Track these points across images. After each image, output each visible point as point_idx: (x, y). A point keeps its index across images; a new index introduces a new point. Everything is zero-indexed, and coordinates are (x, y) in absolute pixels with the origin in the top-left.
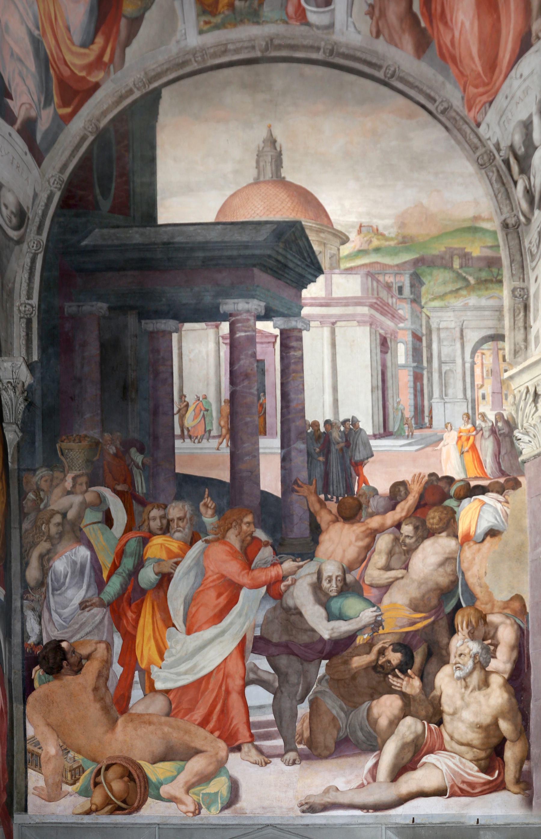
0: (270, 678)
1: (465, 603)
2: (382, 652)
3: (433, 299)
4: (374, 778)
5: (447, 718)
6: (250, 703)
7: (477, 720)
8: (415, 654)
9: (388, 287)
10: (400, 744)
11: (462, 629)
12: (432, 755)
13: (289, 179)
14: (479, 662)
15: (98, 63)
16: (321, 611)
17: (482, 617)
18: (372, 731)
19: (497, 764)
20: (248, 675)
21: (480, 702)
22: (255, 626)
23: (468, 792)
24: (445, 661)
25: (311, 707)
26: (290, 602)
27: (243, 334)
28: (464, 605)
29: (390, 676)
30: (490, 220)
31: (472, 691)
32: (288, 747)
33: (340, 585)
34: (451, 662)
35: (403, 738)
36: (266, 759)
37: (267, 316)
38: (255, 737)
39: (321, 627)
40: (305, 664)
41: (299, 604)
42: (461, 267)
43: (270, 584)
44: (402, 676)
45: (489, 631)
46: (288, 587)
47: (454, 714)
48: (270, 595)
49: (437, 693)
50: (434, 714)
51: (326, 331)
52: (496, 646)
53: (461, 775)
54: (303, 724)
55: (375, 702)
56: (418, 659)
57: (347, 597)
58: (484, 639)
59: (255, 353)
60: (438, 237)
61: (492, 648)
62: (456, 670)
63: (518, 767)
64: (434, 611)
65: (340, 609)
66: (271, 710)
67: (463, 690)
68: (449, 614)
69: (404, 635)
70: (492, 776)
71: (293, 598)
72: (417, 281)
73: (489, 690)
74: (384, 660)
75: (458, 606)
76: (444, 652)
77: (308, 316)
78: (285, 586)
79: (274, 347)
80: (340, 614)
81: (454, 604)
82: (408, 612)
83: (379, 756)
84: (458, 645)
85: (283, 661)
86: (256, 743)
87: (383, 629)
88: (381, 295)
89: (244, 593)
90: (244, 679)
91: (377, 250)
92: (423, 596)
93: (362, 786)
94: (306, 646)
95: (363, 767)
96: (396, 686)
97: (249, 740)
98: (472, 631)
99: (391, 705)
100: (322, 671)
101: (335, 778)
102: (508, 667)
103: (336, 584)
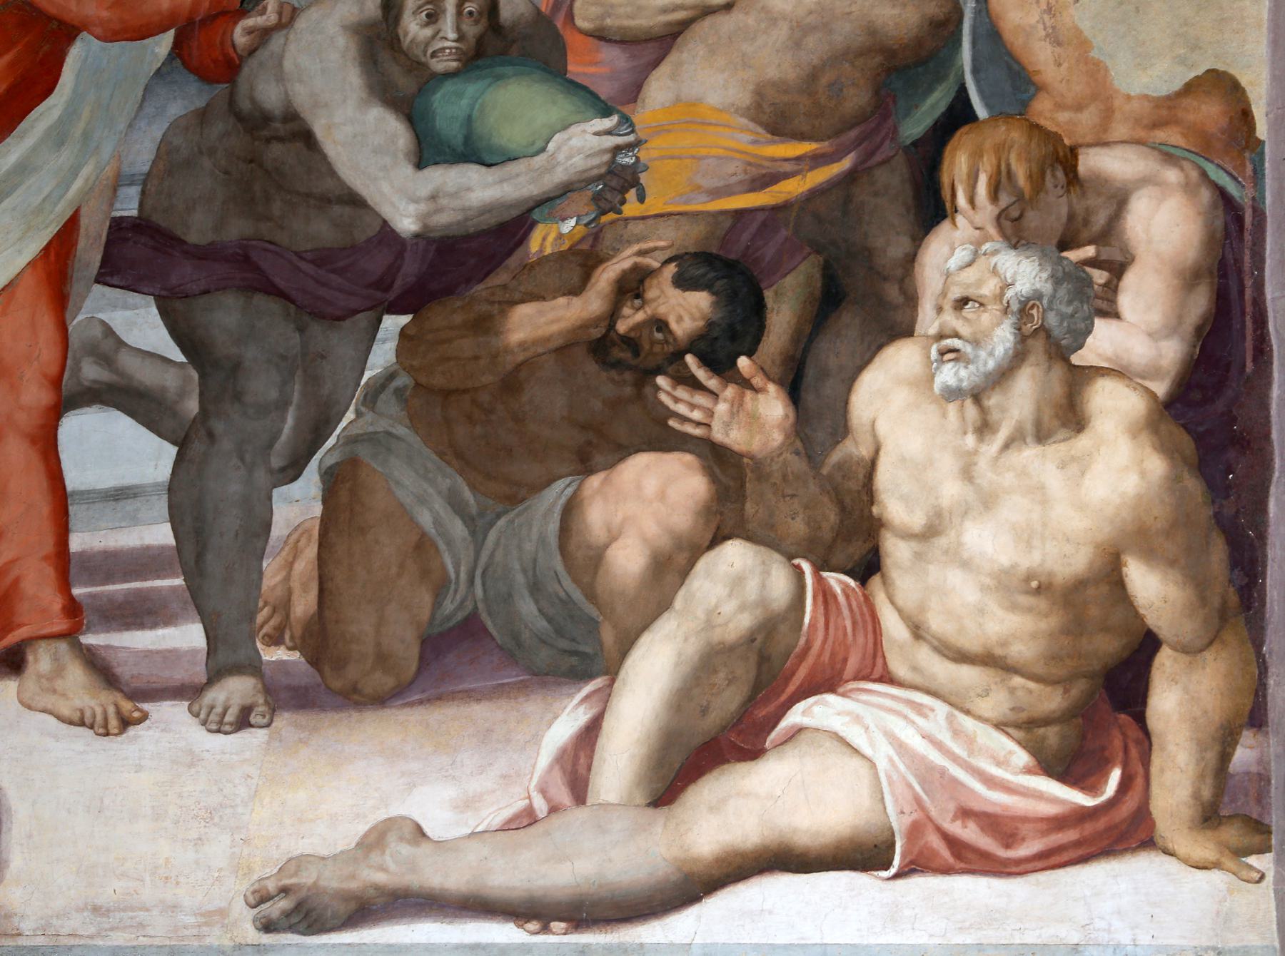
0: (169, 380)
1: (988, 105)
2: (632, 286)
4: (579, 788)
5: (896, 551)
6: (74, 479)
7: (1030, 560)
8: (768, 295)
10: (693, 648)
11: (972, 201)
12: (830, 698)
14: (1043, 330)
16: (390, 128)
17: (1062, 159)
18: (577, 595)
19: (1118, 742)
20: (77, 369)
21: (1042, 488)
22: (118, 182)
23: (985, 855)
24: (894, 324)
25: (329, 496)
26: (269, 95)
28: (981, 112)
29: (661, 381)
31: (1006, 446)
32: (223, 657)
33: (472, 30)
34: (919, 329)
35: (709, 625)
36: (127, 706)
38: (88, 617)
39: (386, 187)
40: (316, 328)
41: (301, 96)
43: (190, 22)
44: (712, 383)
45: (1089, 212)
46: (264, 35)
47: (930, 533)
48: (187, 66)
49: (855, 448)
50: (844, 534)
52: (1118, 270)
53: (955, 782)
54: (290, 565)
55: (595, 481)
56: (782, 317)
57: (499, 78)
58: (1064, 245)
61: (1099, 276)
62: (942, 362)
63: (1211, 756)
64: (853, 134)
65: (469, 119)
66: (161, 506)
67: (970, 440)
68: (915, 144)
69: (728, 223)
70: (1091, 788)
71: (280, 77)
73: (1083, 442)
74: (640, 316)
75: (959, 115)
76: (892, 292)
78: (250, 31)
80: (468, 139)
81: (942, 107)
82: (747, 137)
83: (605, 698)
84: (953, 263)
85: (225, 316)
86: (89, 639)
87: (641, 198)
89: (78, 55)
90: (57, 382)
92: (813, 75)
93: (526, 819)
94: (323, 258)
95: (536, 739)
96: (684, 419)
97: (61, 625)
98: (1015, 214)
99: (662, 496)
100: (382, 355)
101: (411, 786)
102: (1171, 353)
103: (458, 29)
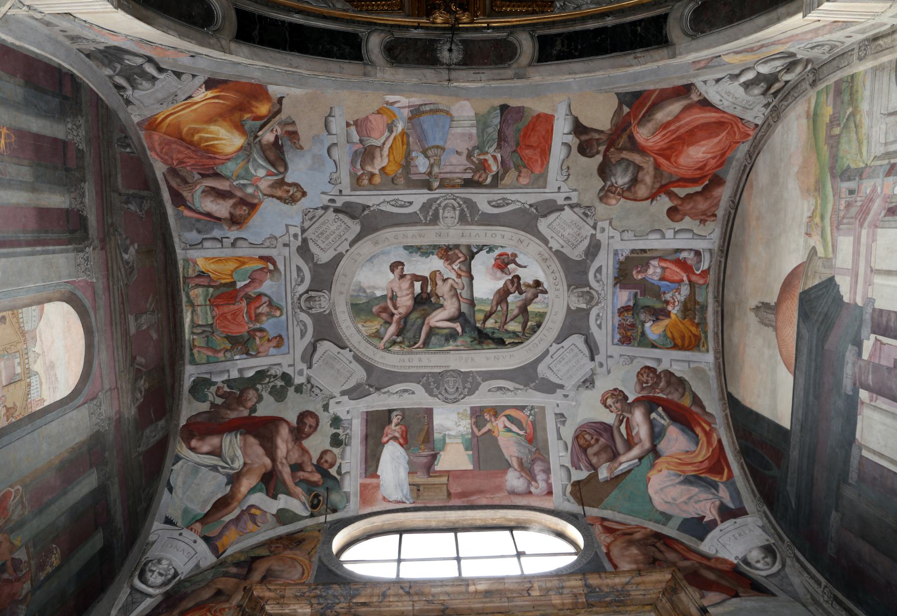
3: (861, 153)
9: (849, 205)
13: (775, 300)
15: (708, 435)
27: (870, 377)
30: (809, 100)
37: (858, 344)
42: (839, 125)
51: (878, 280)
59: (888, 368)
60: (818, 153)
72: (847, 174)
77: (863, 298)
79: (885, 344)
88: (853, 214)
91: (822, 218)
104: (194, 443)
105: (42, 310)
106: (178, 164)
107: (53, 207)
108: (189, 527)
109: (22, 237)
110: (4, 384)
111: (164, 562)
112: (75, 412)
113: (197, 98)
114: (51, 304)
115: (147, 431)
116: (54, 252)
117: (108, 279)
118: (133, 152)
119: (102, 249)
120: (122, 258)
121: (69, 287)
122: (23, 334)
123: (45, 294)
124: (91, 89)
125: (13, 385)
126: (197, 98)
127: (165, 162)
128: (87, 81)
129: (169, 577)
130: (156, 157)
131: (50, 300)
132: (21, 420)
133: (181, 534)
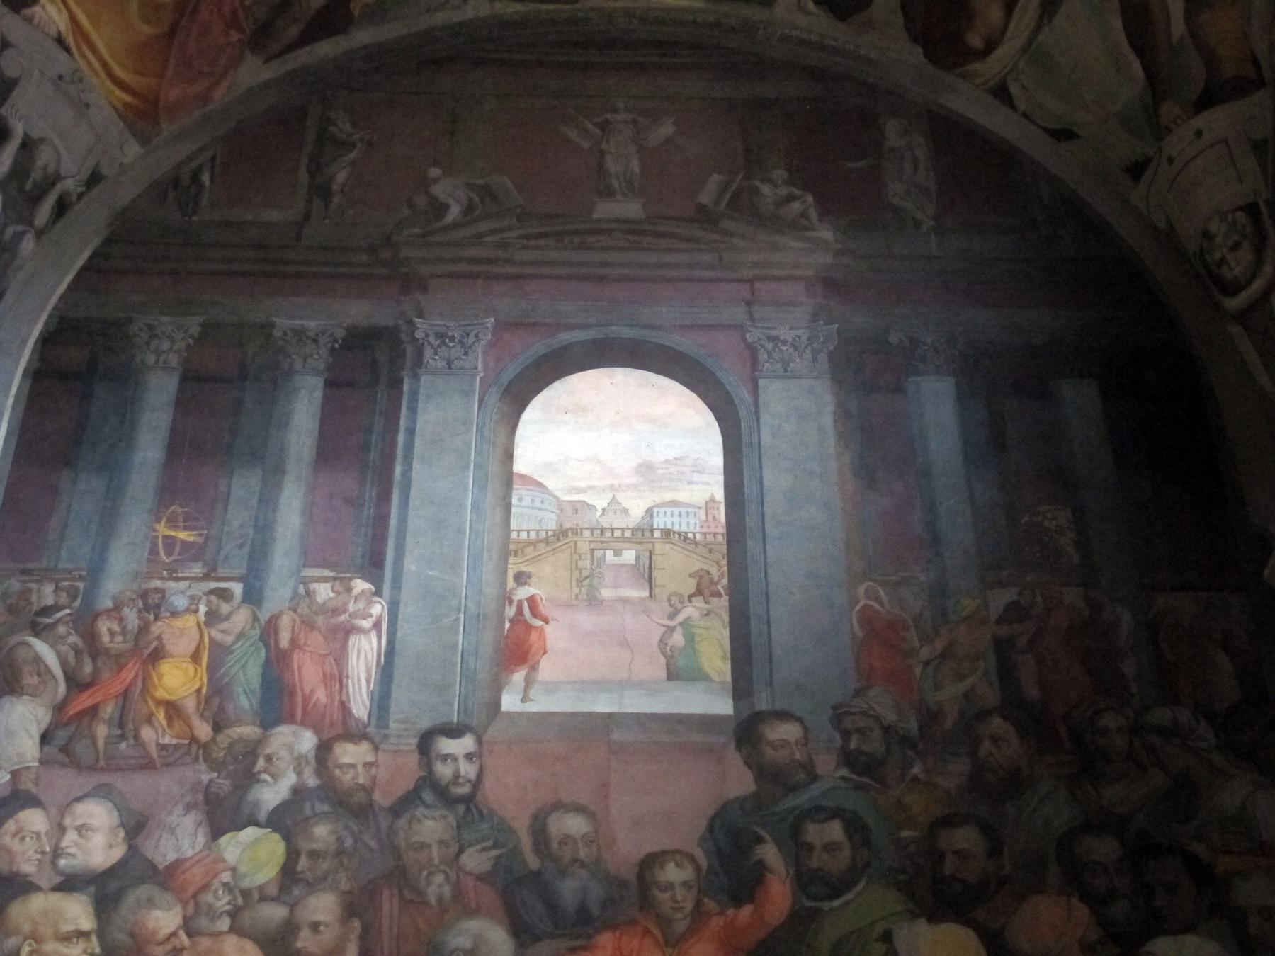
104: (975, 40)
105: (528, 480)
106: (241, 30)
107: (317, 425)
108: (1161, 132)
109: (368, 512)
110: (646, 594)
111: (1213, 227)
112: (764, 418)
113: (60, 21)
114: (518, 452)
115: (895, 191)
116: (411, 432)
117: (496, 277)
118: (213, 159)
119: (424, 289)
120: (456, 226)
121: (493, 397)
122: (561, 533)
123: (494, 468)
124: (69, 288)
125: (656, 574)
126: (60, 21)
127: (235, 62)
128: (54, 300)
129: (1249, 229)
130: (225, 84)
131: (509, 456)
132: (730, 564)
133: (1171, 160)
